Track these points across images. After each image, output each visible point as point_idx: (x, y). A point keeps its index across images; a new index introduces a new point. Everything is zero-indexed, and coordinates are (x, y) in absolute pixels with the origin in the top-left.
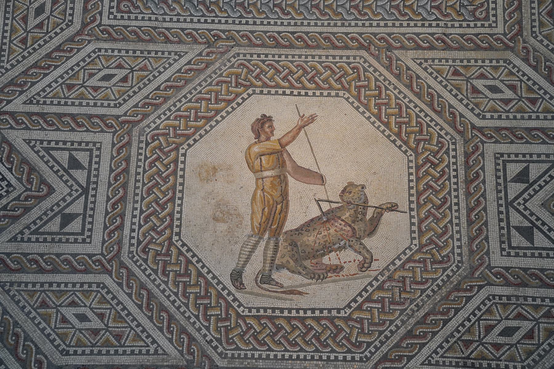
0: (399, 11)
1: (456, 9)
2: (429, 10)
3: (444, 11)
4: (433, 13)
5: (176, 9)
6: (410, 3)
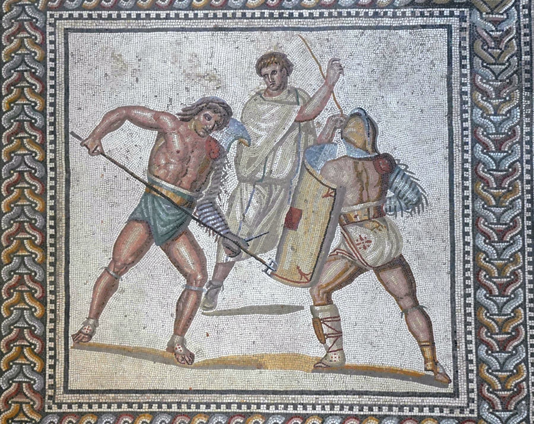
0: (13, 340)
1: (17, 415)
2: (16, 380)
3: (14, 400)
4: (11, 385)
5: (11, 43)
6: (27, 355)
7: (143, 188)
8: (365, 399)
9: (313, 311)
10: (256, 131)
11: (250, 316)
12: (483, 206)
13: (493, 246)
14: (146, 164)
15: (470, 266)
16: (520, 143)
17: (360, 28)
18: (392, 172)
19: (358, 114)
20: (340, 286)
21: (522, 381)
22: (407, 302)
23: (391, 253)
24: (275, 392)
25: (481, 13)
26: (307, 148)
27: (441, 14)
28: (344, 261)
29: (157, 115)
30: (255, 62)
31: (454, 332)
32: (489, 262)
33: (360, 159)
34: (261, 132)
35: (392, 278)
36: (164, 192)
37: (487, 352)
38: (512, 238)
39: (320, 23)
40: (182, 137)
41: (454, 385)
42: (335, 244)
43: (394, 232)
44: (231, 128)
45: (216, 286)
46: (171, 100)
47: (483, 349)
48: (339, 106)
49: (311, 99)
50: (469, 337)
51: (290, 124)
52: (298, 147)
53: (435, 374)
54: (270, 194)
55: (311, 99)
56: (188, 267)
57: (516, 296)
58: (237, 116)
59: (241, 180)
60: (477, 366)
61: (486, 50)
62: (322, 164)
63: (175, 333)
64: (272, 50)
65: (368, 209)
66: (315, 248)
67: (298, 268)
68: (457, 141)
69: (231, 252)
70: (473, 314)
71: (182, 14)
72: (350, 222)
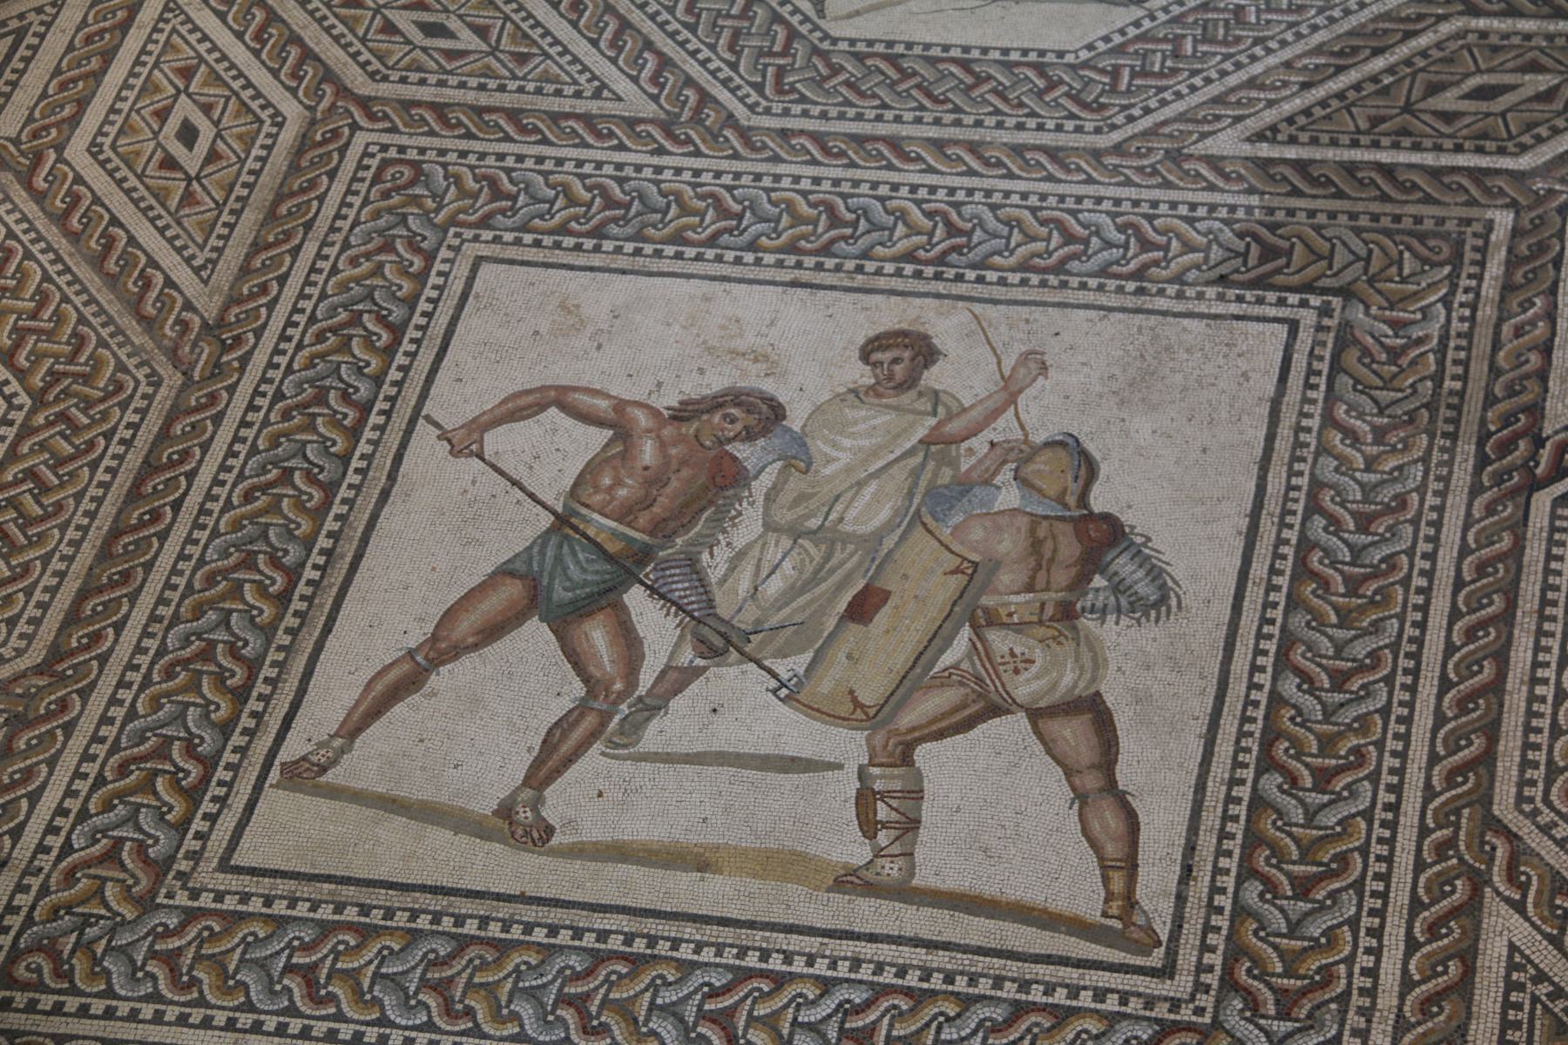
7: (546, 520)
8: (941, 959)
9: (862, 774)
10: (827, 449)
11: (711, 770)
12: (1308, 624)
13: (1317, 698)
14: (568, 482)
15: (1257, 728)
16: (1415, 522)
17: (1101, 308)
18: (1112, 543)
19: (1062, 444)
20: (940, 735)
21: (1337, 963)
22: (1091, 781)
23: (1075, 686)
24: (724, 922)
25: (1367, 307)
26: (931, 492)
27: (1281, 302)
28: (962, 690)
29: (621, 405)
30: (861, 341)
31: (1190, 848)
32: (1302, 725)
33: (1046, 517)
34: (837, 455)
35: (1067, 733)
36: (591, 532)
37: (1261, 895)
38: (1363, 687)
39: (1018, 294)
40: (662, 445)
41: (1167, 953)
42: (947, 659)
43: (1091, 649)
44: (776, 441)
45: (653, 706)
46: (659, 385)
47: (1252, 890)
48: (1022, 427)
49: (965, 410)
50: (1224, 862)
51: (908, 445)
52: (915, 484)
53: (1126, 926)
54: (827, 559)
55: (965, 410)
56: (600, 666)
57: (1354, 795)
58: (795, 421)
59: (768, 526)
60: (1232, 921)
61: (1368, 366)
62: (959, 518)
63: (527, 782)
64: (904, 326)
65: (1043, 605)
66: (901, 660)
67: (852, 692)
68: (1272, 506)
69: (704, 649)
70: (1243, 818)
71: (730, 256)
72: (993, 620)
